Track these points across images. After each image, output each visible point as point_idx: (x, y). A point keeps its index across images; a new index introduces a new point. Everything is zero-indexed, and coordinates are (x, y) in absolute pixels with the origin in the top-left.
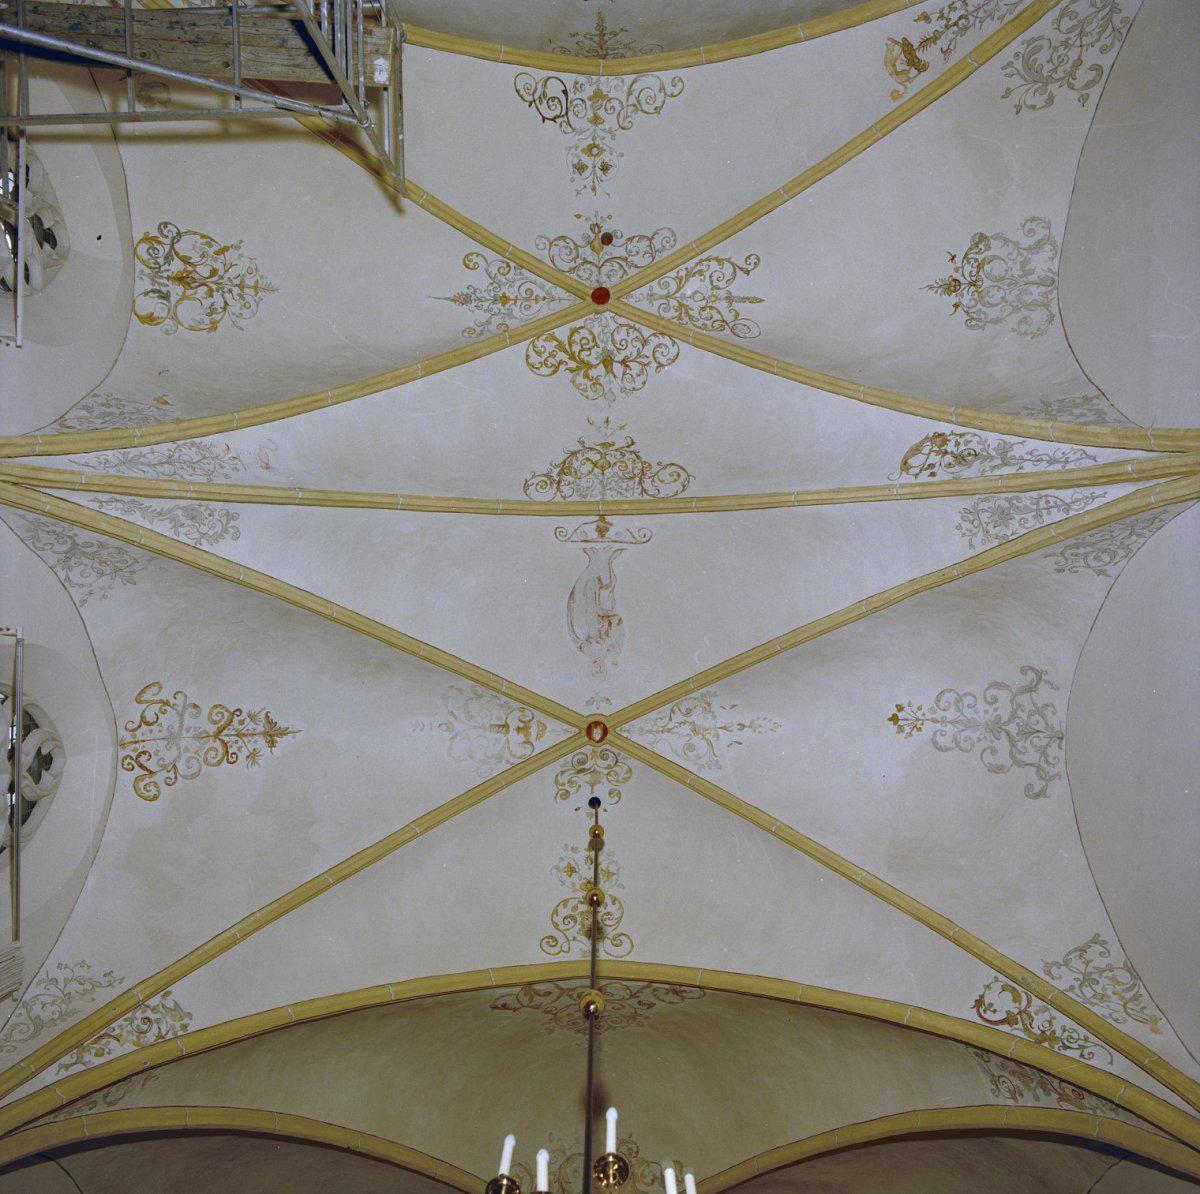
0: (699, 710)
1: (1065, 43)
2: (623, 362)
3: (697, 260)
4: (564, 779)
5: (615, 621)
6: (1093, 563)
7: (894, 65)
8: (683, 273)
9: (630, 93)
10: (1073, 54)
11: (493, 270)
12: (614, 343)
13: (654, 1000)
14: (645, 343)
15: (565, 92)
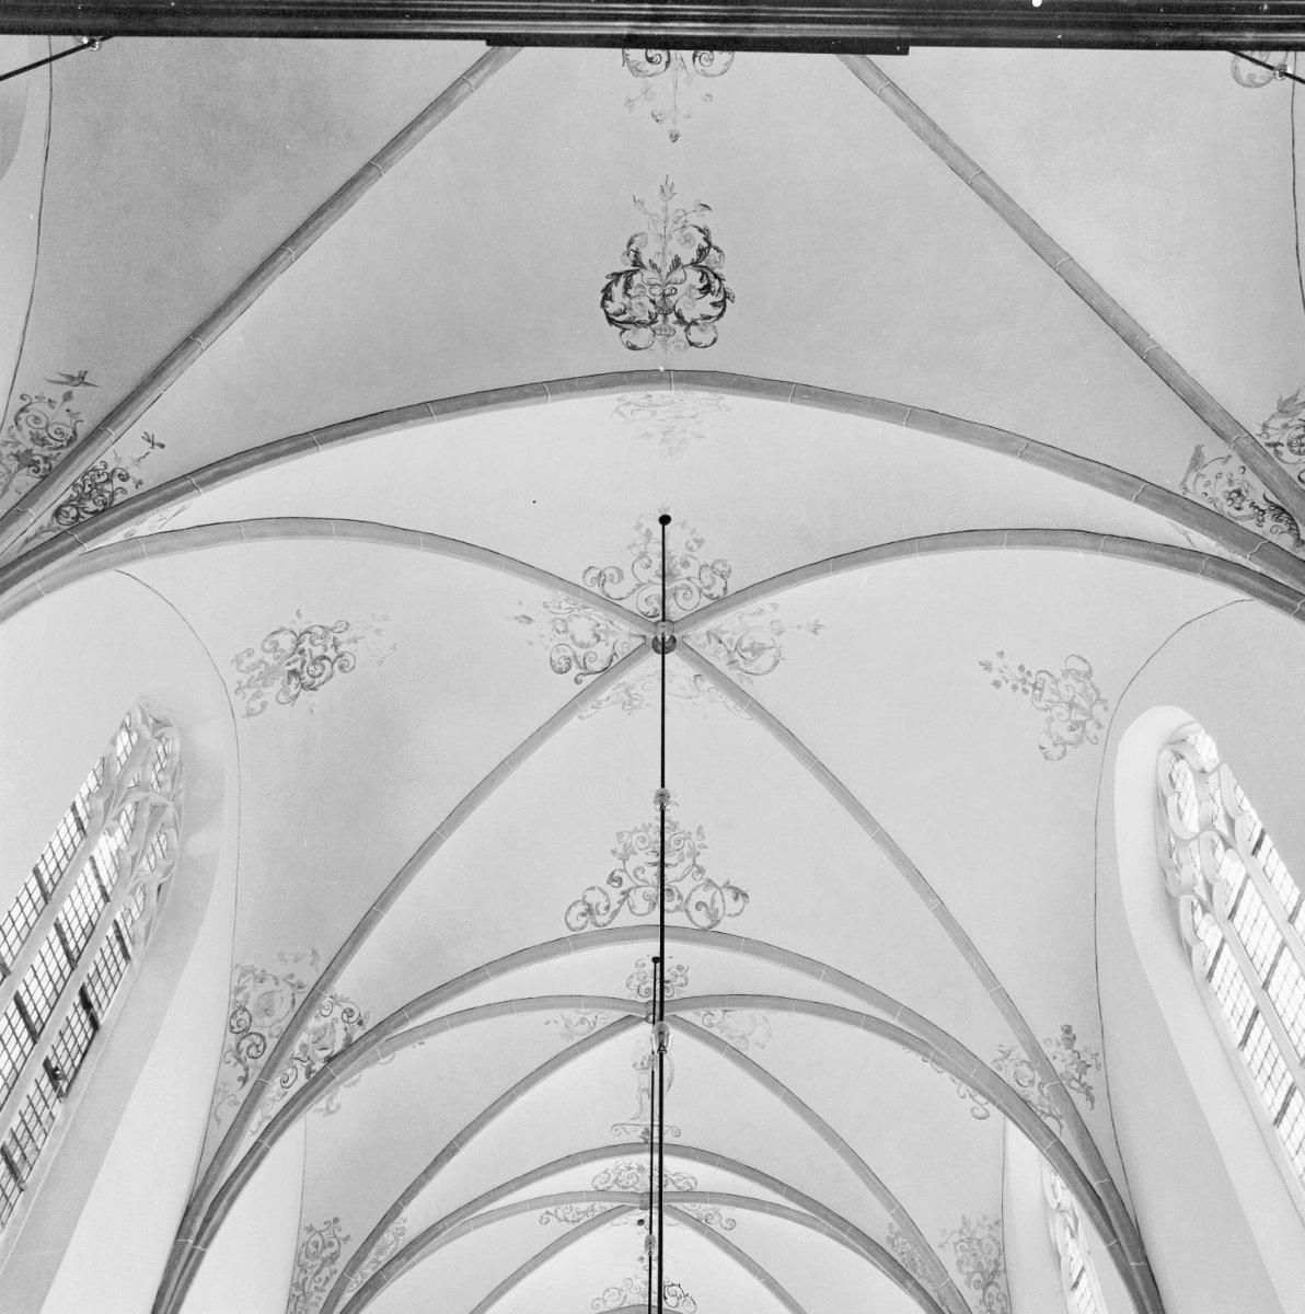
0: (575, 1022)
2: (630, 1168)
3: (581, 1222)
4: (682, 980)
5: (639, 1066)
6: (317, 1238)
8: (590, 1214)
9: (625, 1297)
11: (716, 1218)
12: (637, 1177)
13: (608, 888)
14: (616, 1181)
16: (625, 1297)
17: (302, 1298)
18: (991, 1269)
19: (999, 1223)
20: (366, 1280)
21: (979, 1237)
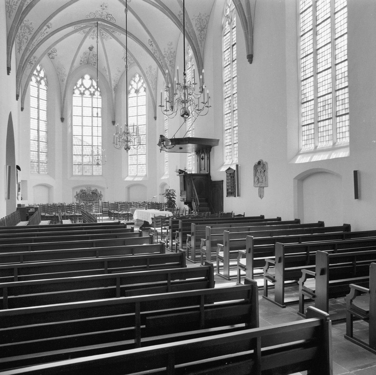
1: (25, 33)
7: (51, 24)
9: (96, 16)
10: (22, 31)
15: (107, 18)
16: (96, 16)
17: (10, 7)
18: (204, 27)
19: (209, 16)
20: (28, 4)
21: (202, 19)
